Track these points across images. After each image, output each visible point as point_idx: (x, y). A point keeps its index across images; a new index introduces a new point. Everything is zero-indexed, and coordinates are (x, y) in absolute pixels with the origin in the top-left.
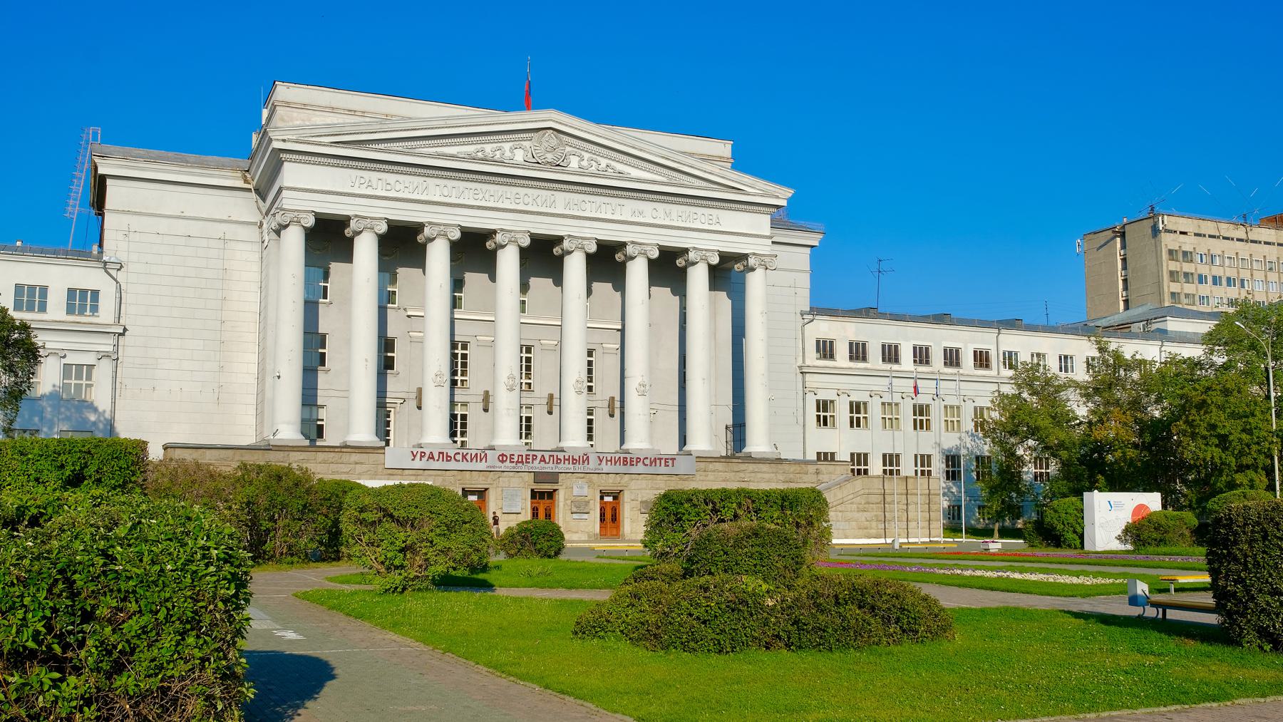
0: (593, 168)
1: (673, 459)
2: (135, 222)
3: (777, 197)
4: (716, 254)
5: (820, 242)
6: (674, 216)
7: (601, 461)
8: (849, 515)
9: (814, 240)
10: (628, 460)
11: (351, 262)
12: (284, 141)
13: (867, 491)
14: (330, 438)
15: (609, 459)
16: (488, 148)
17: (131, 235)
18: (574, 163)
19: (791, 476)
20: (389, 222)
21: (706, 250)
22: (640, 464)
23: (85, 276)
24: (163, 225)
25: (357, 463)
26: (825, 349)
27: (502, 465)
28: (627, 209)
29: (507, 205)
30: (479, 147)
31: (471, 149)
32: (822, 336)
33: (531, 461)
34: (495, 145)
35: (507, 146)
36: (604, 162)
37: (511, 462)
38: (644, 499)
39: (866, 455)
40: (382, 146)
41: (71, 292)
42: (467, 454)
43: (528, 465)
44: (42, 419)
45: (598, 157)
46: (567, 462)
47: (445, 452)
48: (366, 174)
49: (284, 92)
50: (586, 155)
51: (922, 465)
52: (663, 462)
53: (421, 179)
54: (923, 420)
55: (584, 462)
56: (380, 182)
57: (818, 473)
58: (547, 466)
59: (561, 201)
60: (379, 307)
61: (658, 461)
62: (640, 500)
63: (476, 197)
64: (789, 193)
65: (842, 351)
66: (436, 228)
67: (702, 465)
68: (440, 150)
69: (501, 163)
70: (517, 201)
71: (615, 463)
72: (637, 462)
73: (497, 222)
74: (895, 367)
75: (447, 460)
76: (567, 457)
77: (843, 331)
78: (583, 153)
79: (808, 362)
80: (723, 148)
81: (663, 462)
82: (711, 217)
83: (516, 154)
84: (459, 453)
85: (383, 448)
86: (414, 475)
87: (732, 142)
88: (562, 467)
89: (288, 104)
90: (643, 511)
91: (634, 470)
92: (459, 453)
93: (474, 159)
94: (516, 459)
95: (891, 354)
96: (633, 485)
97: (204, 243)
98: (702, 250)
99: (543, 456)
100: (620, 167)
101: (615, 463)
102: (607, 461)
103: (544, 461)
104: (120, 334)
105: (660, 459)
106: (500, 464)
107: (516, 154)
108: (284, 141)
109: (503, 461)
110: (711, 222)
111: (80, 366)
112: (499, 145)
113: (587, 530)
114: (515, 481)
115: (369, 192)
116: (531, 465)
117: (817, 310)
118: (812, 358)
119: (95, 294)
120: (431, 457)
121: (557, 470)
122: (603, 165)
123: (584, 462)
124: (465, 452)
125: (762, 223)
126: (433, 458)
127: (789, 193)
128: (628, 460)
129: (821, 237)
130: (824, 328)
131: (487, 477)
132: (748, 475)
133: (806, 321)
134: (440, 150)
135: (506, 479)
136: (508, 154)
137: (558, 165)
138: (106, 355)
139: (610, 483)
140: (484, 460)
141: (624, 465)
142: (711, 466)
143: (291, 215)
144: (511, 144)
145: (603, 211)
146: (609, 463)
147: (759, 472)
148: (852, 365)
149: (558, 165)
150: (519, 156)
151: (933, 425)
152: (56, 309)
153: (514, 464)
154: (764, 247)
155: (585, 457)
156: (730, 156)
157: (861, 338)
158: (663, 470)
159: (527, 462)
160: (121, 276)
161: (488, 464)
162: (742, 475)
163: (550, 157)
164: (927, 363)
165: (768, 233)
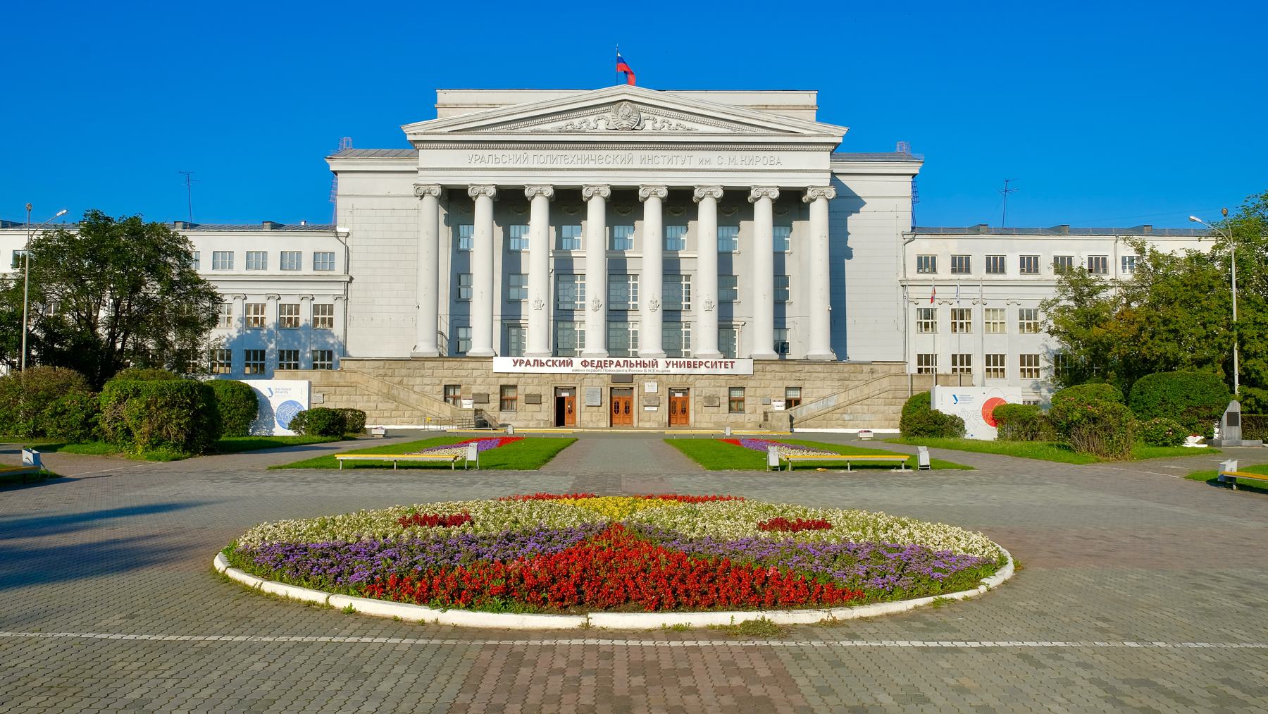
0: (665, 128)
1: (732, 362)
2: (358, 203)
3: (833, 136)
4: (665, 188)
5: (920, 170)
6: (738, 160)
7: (668, 365)
8: (876, 408)
9: (915, 168)
10: (692, 364)
11: (643, 220)
12: (415, 134)
13: (894, 387)
14: (794, 353)
15: (675, 362)
16: (576, 122)
17: (355, 212)
18: (649, 126)
19: (846, 375)
20: (497, 187)
21: (766, 187)
22: (703, 367)
23: (323, 242)
24: (376, 203)
25: (473, 369)
26: (927, 264)
27: (585, 369)
28: (696, 158)
29: (592, 165)
30: (568, 122)
31: (562, 124)
32: (992, 253)
33: (608, 365)
34: (581, 119)
35: (591, 119)
36: (674, 122)
37: (592, 366)
38: (707, 395)
39: (1002, 357)
40: (490, 130)
42: (557, 361)
43: (607, 368)
44: (299, 343)
45: (670, 119)
46: (639, 366)
47: (539, 359)
48: (479, 152)
49: (443, 96)
50: (659, 119)
51: (962, 364)
52: (723, 364)
53: (522, 152)
54: (928, 323)
55: (653, 366)
56: (489, 157)
57: (873, 373)
58: (622, 369)
59: (638, 158)
60: (774, 253)
61: (718, 364)
62: (704, 395)
63: (566, 161)
64: (843, 130)
65: (944, 266)
66: (761, 190)
67: (760, 367)
68: (536, 128)
69: (579, 132)
70: (600, 161)
71: (680, 367)
72: (700, 365)
73: (695, 180)
74: (1000, 277)
75: (541, 366)
76: (639, 362)
77: (944, 248)
78: (656, 117)
79: (909, 276)
80: (810, 98)
81: (723, 364)
82: (772, 159)
83: (600, 124)
84: (550, 360)
85: (492, 357)
86: (517, 377)
87: (817, 92)
88: (635, 370)
89: (444, 106)
90: (705, 404)
91: (697, 371)
92: (550, 360)
93: (560, 132)
94: (595, 365)
95: (996, 265)
96: (698, 384)
97: (404, 213)
98: (763, 187)
99: (618, 361)
100: (689, 125)
101: (680, 367)
102: (673, 364)
103: (620, 365)
104: (348, 282)
105: (721, 362)
106: (583, 368)
107: (600, 124)
108: (415, 134)
109: (585, 366)
110: (772, 163)
111: (324, 306)
112: (584, 118)
113: (657, 419)
114: (597, 382)
115: (483, 166)
116: (608, 368)
117: (916, 230)
118: (912, 273)
120: (528, 363)
121: (631, 373)
122: (674, 125)
123: (653, 366)
124: (555, 359)
125: (822, 160)
126: (530, 364)
127: (843, 130)
128: (692, 364)
129: (921, 165)
130: (925, 245)
131: (574, 378)
132: (804, 374)
133: (907, 240)
134: (536, 128)
135: (589, 380)
136: (593, 125)
137: (634, 129)
138: (337, 298)
139: (676, 383)
140: (683, 366)
141: (688, 367)
142: (768, 368)
143: (592, 189)
144: (595, 117)
145: (674, 163)
146: (675, 366)
147: (814, 372)
148: (955, 276)
149: (634, 129)
150: (602, 126)
151: (938, 327)
152: (239, 267)
153: (594, 368)
155: (654, 362)
156: (815, 104)
157: (964, 252)
158: (723, 371)
159: (605, 366)
160: (349, 241)
161: (574, 368)
162: (798, 374)
163: (625, 123)
164: (1036, 271)
165: (828, 168)
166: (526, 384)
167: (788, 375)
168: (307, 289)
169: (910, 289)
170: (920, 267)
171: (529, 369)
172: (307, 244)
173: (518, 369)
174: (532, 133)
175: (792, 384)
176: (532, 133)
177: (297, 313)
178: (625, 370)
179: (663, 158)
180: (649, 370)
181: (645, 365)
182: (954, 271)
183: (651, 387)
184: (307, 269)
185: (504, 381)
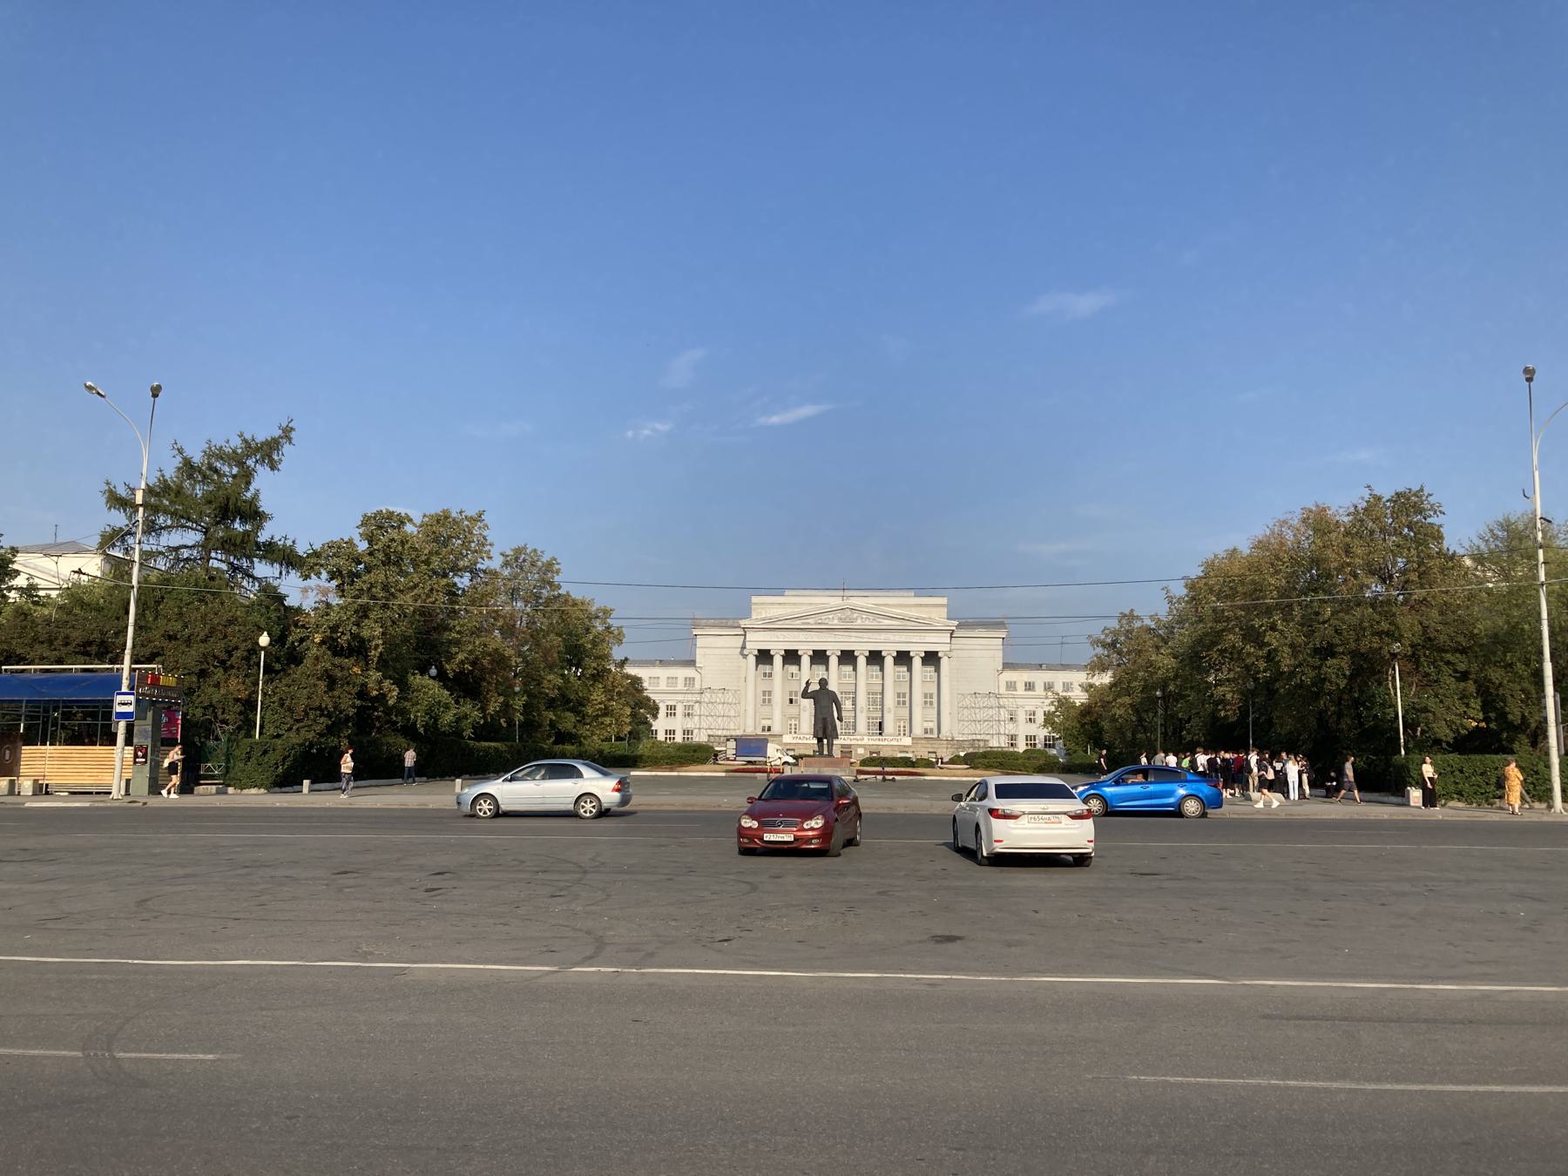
2: (708, 651)
24: (717, 651)
26: (1011, 686)
28: (883, 636)
41: (686, 679)
56: (780, 635)
59: (854, 636)
69: (825, 624)
80: (944, 601)
88: (853, 742)
89: (756, 604)
96: (885, 749)
117: (1007, 666)
118: (1003, 690)
119: (694, 679)
125: (946, 637)
130: (1010, 676)
138: (697, 702)
154: (947, 648)
160: (702, 672)
166: (799, 749)
167: (929, 746)
168: (680, 697)
169: (1001, 700)
170: (1007, 687)
171: (800, 741)
172: (682, 673)
173: (795, 741)
174: (803, 624)
175: (931, 750)
176: (803, 624)
177: (675, 710)
178: (848, 742)
179: (866, 636)
180: (860, 743)
181: (858, 740)
182: (1026, 690)
183: (861, 751)
184: (680, 686)
185: (788, 747)
